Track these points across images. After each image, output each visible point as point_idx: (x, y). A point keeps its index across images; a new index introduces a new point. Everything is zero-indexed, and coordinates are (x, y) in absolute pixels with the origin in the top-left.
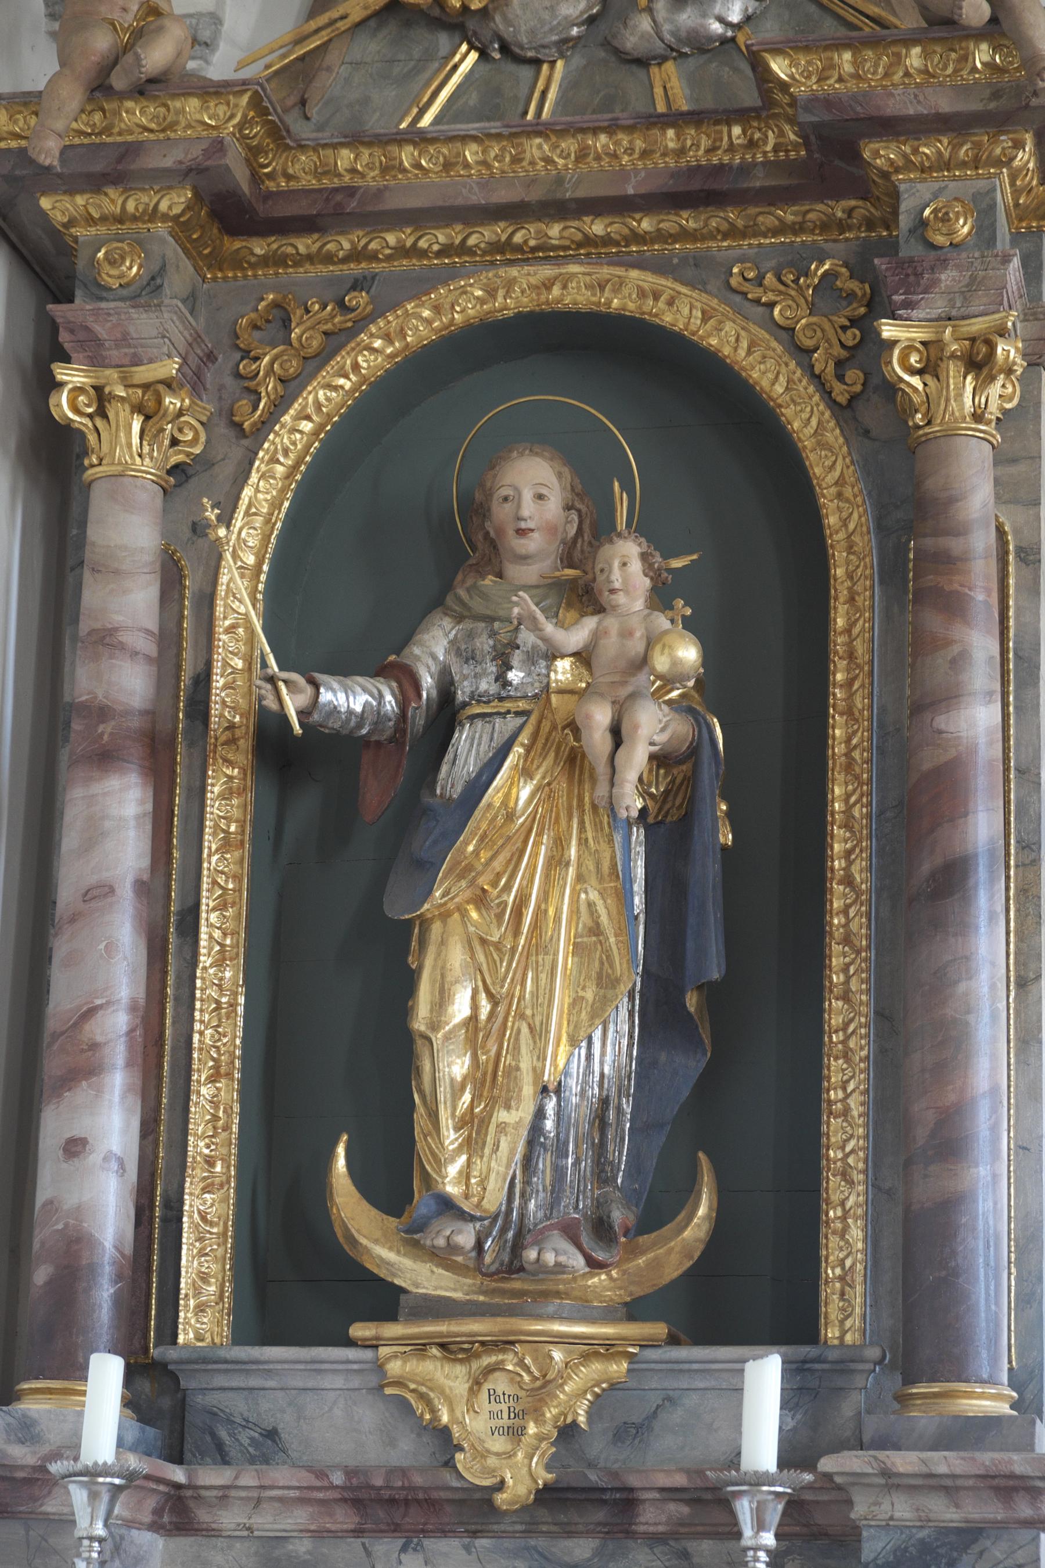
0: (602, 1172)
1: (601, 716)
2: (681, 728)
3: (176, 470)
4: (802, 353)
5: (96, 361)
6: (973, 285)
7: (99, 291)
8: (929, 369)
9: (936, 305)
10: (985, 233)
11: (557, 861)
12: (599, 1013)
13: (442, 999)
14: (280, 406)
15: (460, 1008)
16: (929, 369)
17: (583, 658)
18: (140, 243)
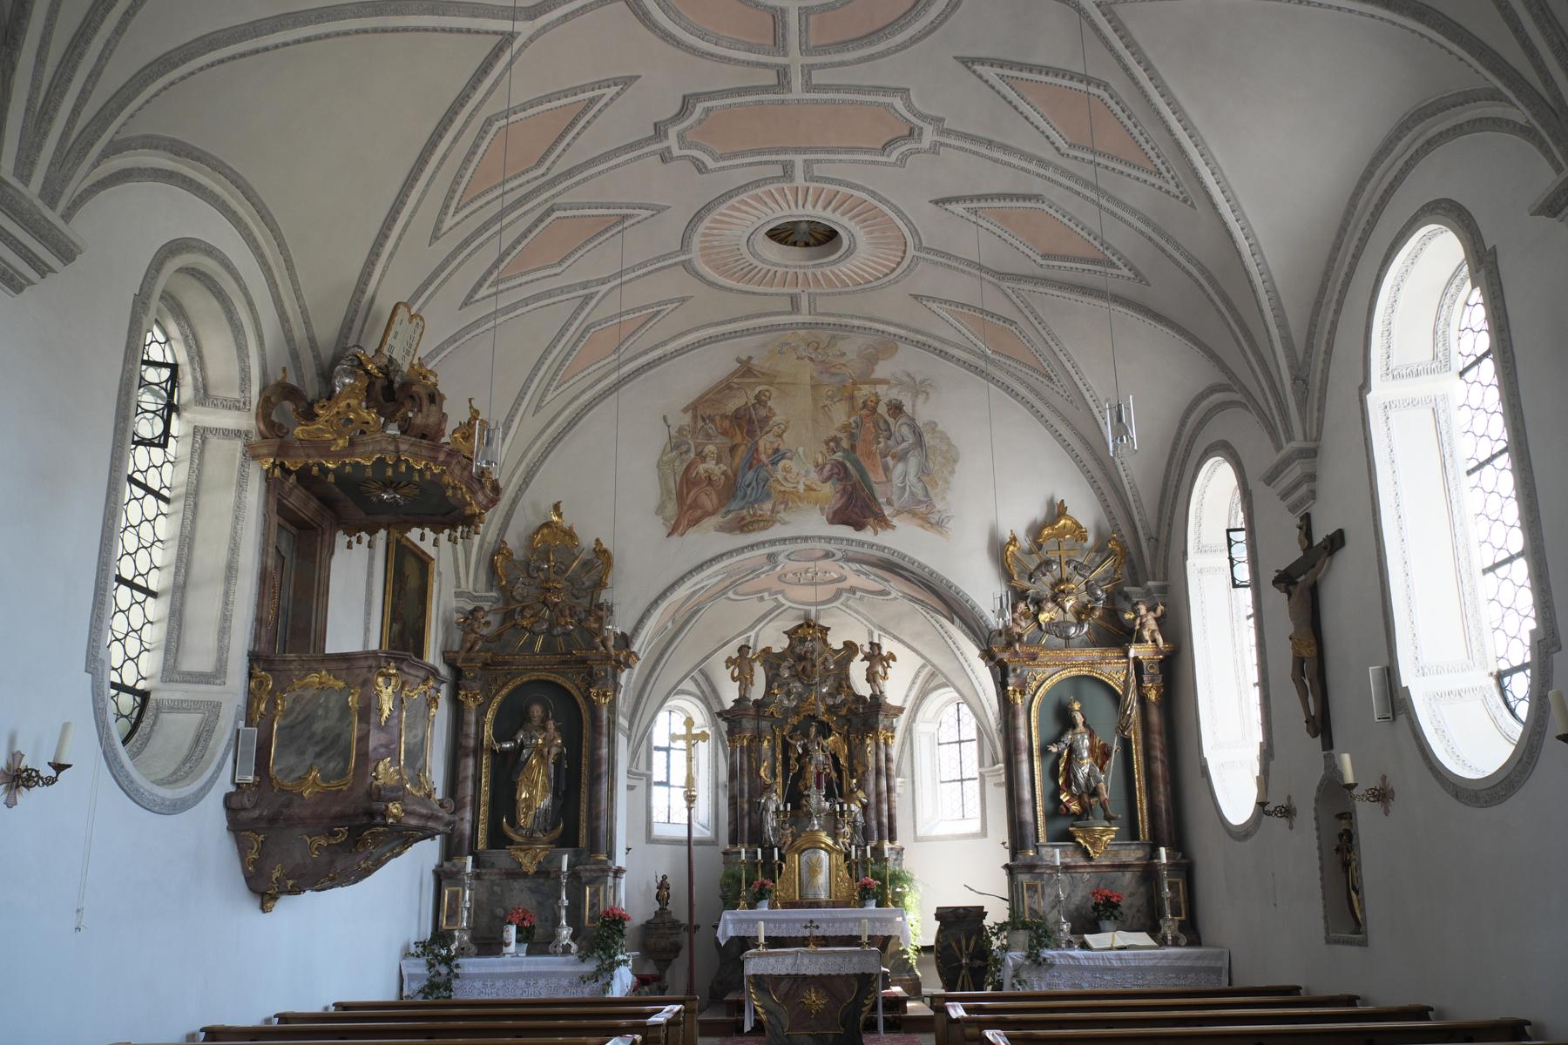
0: (546, 820)
1: (546, 750)
2: (559, 750)
3: (479, 705)
4: (579, 689)
5: (466, 690)
6: (604, 684)
7: (467, 679)
8: (597, 696)
9: (598, 686)
10: (606, 675)
11: (539, 772)
12: (545, 797)
13: (521, 794)
14: (496, 694)
15: (523, 796)
16: (597, 696)
17: (544, 739)
18: (473, 671)
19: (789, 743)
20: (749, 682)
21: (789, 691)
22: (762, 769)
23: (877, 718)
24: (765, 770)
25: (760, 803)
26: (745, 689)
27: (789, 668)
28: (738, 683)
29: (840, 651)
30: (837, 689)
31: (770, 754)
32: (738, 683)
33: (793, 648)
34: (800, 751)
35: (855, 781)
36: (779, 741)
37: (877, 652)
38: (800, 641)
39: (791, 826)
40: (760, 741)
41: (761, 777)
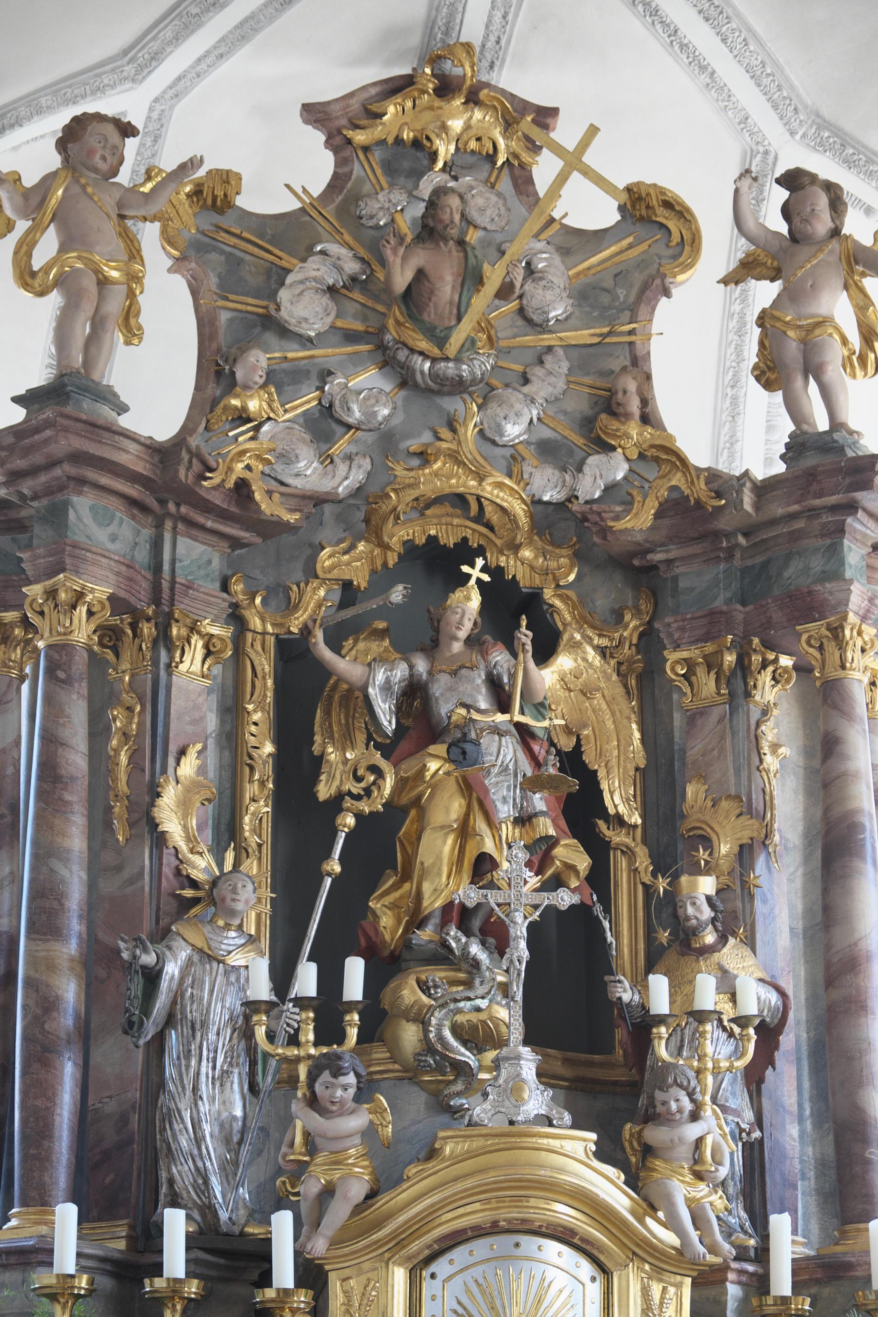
19: (324, 672)
20: (115, 304)
21: (327, 410)
22: (169, 796)
23: (835, 552)
24: (184, 805)
25: (152, 977)
26: (93, 341)
27: (331, 290)
28: (55, 299)
29: (599, 237)
30: (587, 425)
31: (212, 722)
32: (55, 299)
33: (356, 198)
34: (388, 722)
35: (707, 885)
36: (265, 664)
37: (823, 225)
38: (390, 169)
39: (364, 1094)
40: (163, 638)
41: (160, 839)
